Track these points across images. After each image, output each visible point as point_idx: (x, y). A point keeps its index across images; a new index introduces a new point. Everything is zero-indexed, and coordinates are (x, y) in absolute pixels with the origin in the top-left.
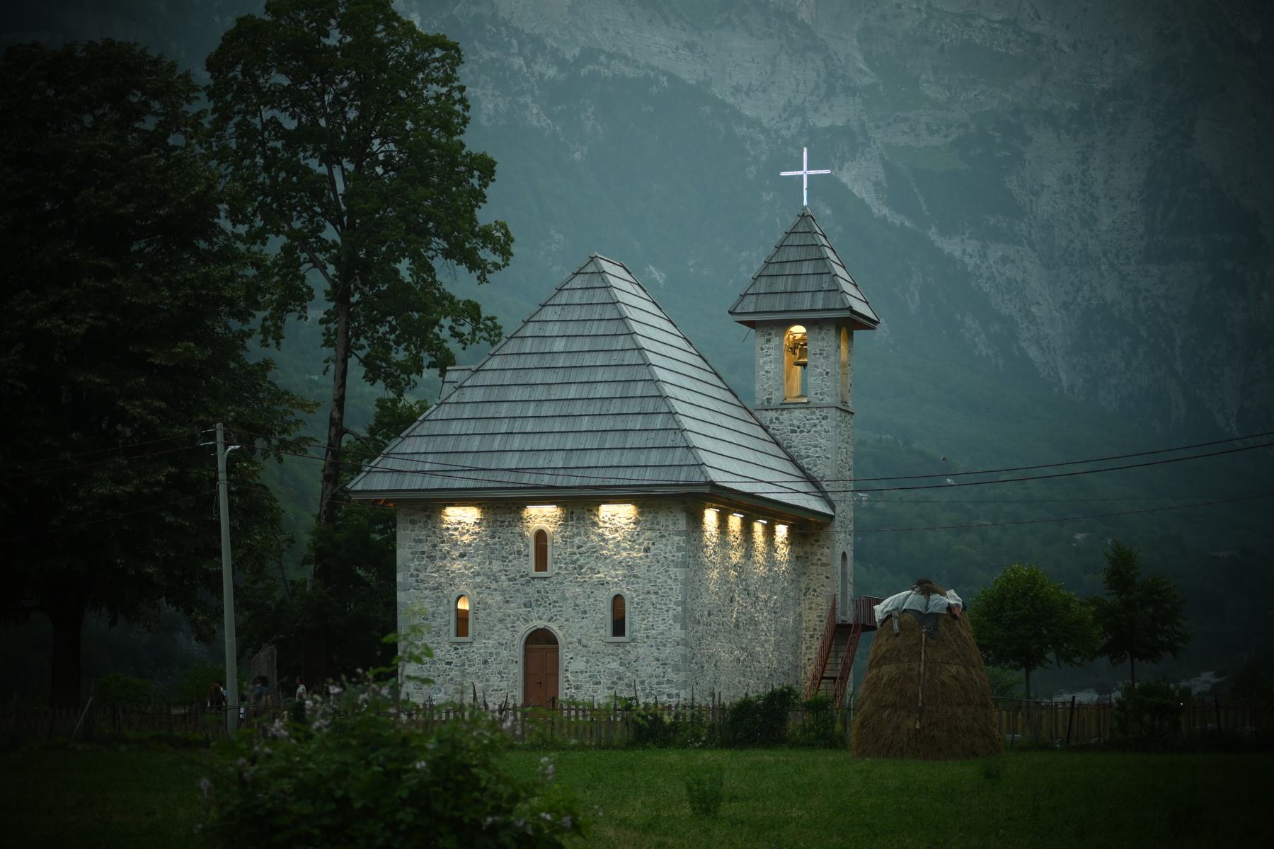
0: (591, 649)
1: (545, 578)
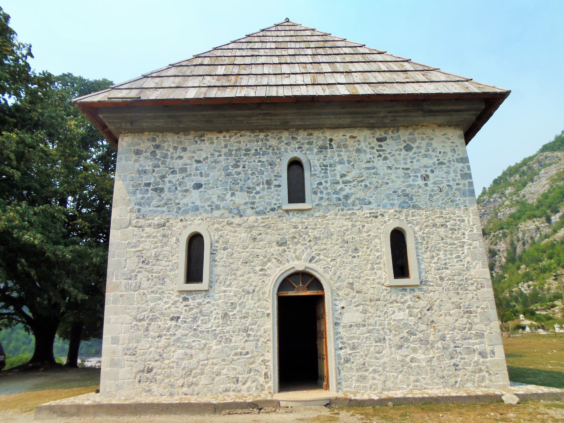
0: (368, 296)
1: (302, 211)
